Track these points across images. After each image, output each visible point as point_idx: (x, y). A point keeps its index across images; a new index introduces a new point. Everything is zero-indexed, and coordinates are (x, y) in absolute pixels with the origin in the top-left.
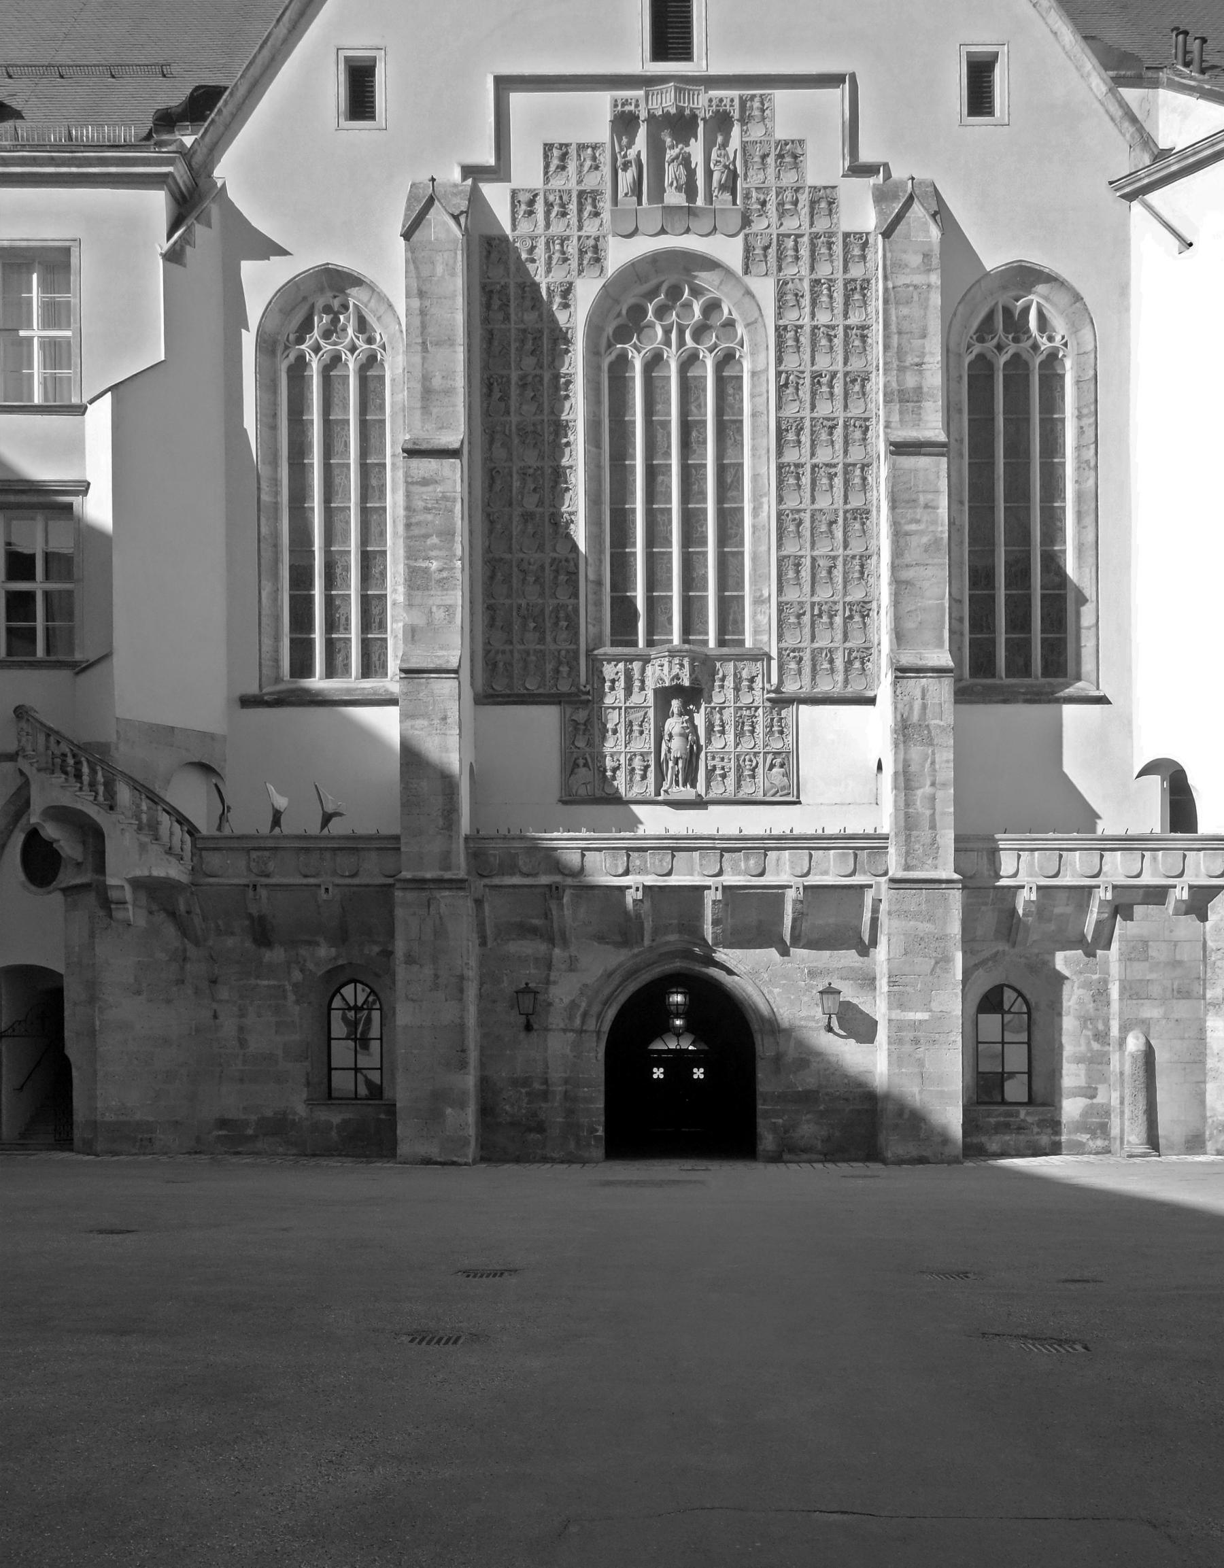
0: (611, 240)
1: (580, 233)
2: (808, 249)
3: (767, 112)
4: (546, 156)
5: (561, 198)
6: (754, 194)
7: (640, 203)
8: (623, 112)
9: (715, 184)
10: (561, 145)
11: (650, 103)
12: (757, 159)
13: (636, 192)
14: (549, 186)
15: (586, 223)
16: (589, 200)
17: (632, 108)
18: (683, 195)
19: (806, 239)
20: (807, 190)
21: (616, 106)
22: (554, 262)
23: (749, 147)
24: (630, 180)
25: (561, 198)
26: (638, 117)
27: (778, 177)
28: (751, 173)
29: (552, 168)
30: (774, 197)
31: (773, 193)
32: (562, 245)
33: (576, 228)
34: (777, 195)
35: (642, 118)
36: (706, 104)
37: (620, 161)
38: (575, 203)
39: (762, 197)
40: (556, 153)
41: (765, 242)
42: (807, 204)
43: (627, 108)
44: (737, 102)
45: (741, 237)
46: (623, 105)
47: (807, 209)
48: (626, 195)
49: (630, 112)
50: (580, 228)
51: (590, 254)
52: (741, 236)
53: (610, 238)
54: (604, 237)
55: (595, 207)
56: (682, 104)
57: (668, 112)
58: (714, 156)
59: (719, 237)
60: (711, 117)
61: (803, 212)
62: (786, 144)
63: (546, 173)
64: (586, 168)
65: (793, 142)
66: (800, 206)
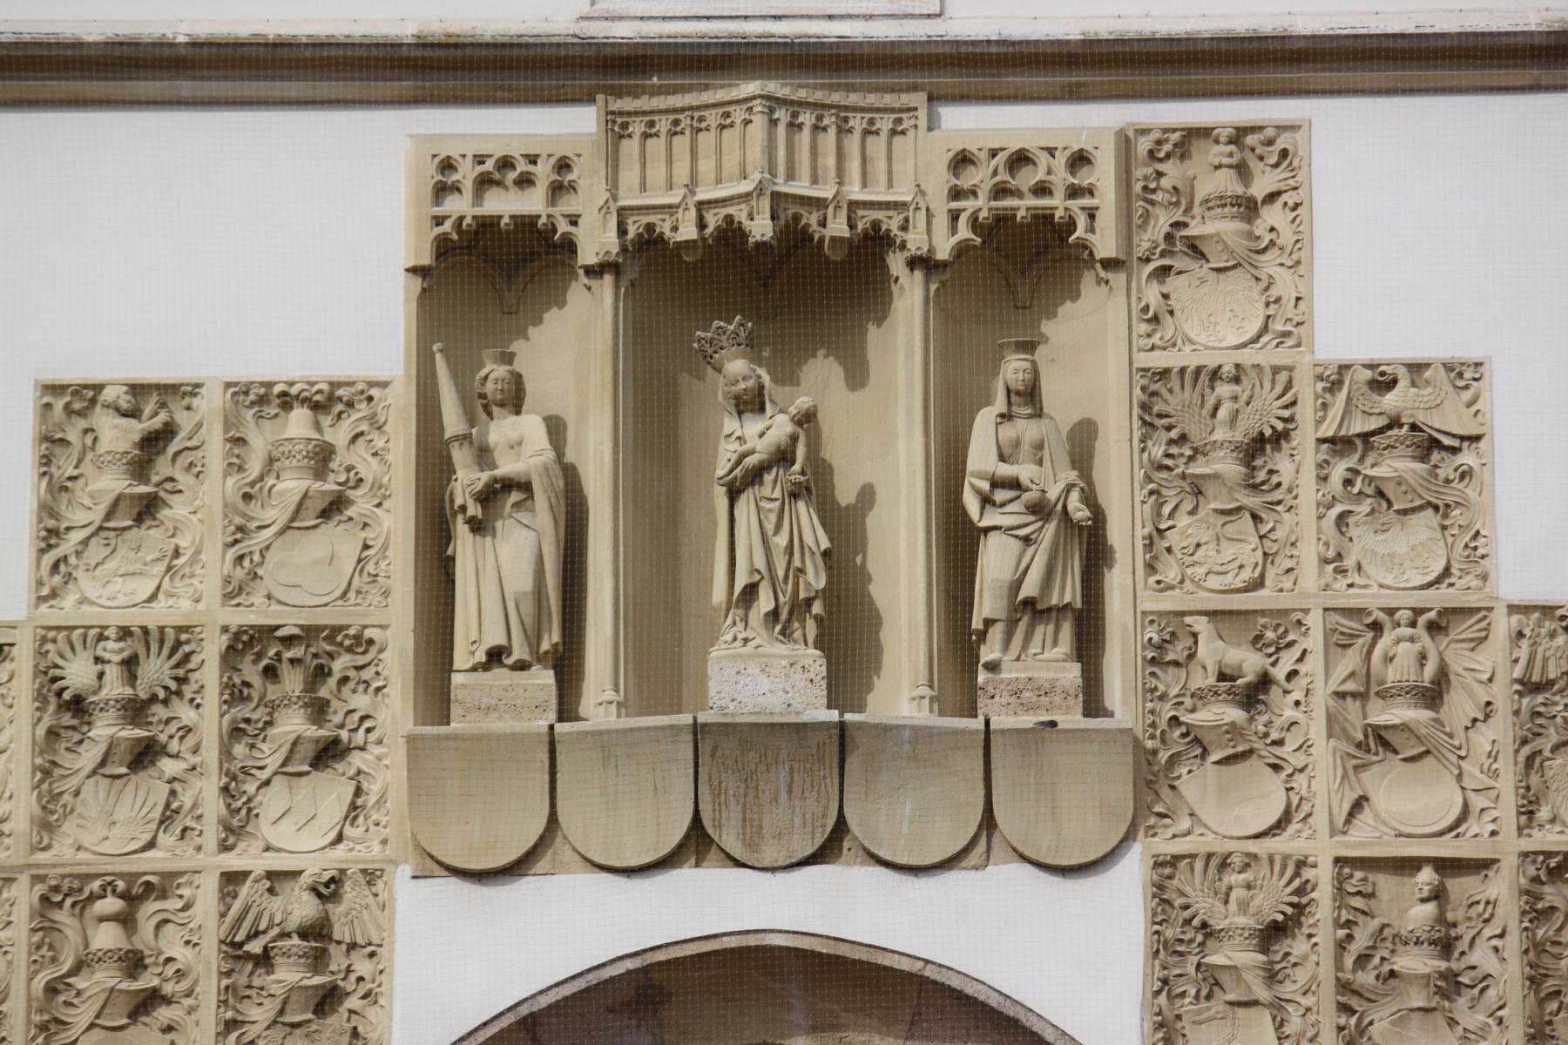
0: (403, 885)
1: (233, 861)
2: (1513, 944)
3: (1272, 215)
4: (51, 443)
5: (130, 665)
6: (1213, 650)
7: (567, 710)
8: (487, 225)
9: (987, 603)
10: (138, 390)
11: (629, 176)
12: (1227, 466)
13: (552, 637)
14: (67, 610)
15: (272, 802)
16: (293, 681)
17: (532, 203)
18: (814, 660)
19: (1502, 888)
20: (1502, 625)
21: (442, 191)
22: (81, 1016)
23: (1175, 401)
24: (520, 581)
25: (130, 665)
26: (569, 246)
27: (1335, 562)
28: (1185, 529)
29: (82, 514)
30: (1314, 664)
31: (1314, 641)
32: (126, 920)
33: (211, 834)
34: (1339, 642)
35: (588, 254)
36: (938, 181)
37: (467, 479)
38: (212, 697)
39: (1251, 662)
40: (117, 435)
41: (1271, 901)
42: (1502, 695)
43: (504, 204)
44: (1103, 175)
45: (1132, 870)
46: (485, 182)
47: (1499, 732)
48: (496, 656)
49: (526, 224)
50: (233, 832)
51: (288, 974)
52: (1132, 870)
53: (403, 885)
54: (371, 877)
55: (318, 710)
56: (801, 187)
57: (732, 234)
58: (981, 457)
59: (1007, 876)
60: (962, 250)
61: (1482, 739)
62: (1383, 383)
63: (50, 536)
64: (274, 514)
65: (1416, 368)
66: (1459, 706)
